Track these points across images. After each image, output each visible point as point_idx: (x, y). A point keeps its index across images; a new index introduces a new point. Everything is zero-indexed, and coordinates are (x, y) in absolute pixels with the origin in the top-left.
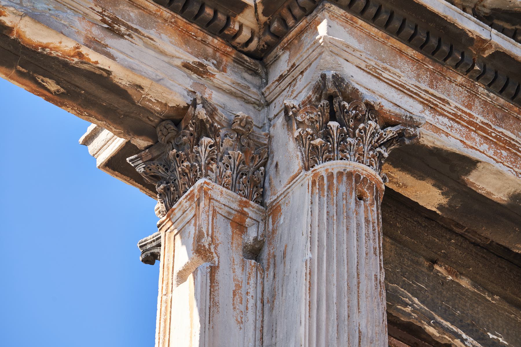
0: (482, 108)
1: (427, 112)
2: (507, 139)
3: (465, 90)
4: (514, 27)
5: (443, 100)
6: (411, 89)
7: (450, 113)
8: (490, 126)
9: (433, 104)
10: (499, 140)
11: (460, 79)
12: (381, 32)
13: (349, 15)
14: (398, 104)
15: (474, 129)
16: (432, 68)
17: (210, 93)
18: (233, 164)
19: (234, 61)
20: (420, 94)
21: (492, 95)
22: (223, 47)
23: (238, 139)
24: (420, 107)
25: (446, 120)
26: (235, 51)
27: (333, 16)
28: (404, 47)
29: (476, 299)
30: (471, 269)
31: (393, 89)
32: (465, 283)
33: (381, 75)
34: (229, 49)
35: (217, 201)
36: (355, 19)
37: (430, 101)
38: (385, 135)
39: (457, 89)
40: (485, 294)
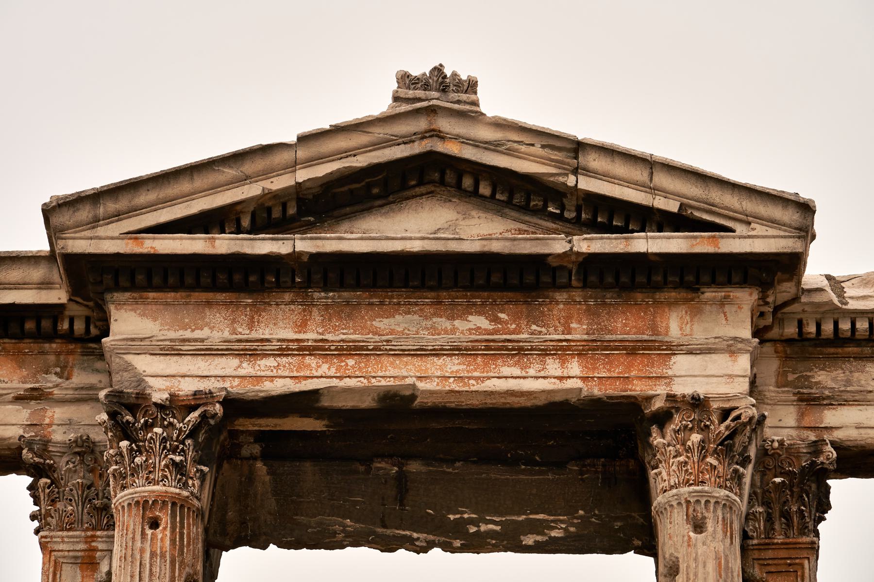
0: (322, 316)
1: (245, 365)
2: (351, 344)
3: (298, 305)
4: (363, 184)
5: (262, 340)
6: (220, 347)
7: (274, 350)
8: (326, 341)
9: (250, 350)
10: (342, 349)
11: (288, 297)
12: (179, 294)
13: (135, 295)
14: (205, 374)
15: (308, 353)
16: (251, 301)
17: (51, 414)
18: (76, 495)
19: (83, 355)
20: (232, 347)
21: (331, 294)
22: (64, 348)
23: (82, 462)
24: (234, 362)
25: (271, 362)
26: (79, 345)
27: (120, 304)
28: (211, 295)
29: (432, 478)
30: (428, 440)
31: (200, 358)
32: (414, 467)
33: (181, 350)
34: (72, 347)
35: (59, 551)
36: (145, 294)
37: (246, 350)
38: (185, 427)
39: (287, 310)
40: (442, 468)
